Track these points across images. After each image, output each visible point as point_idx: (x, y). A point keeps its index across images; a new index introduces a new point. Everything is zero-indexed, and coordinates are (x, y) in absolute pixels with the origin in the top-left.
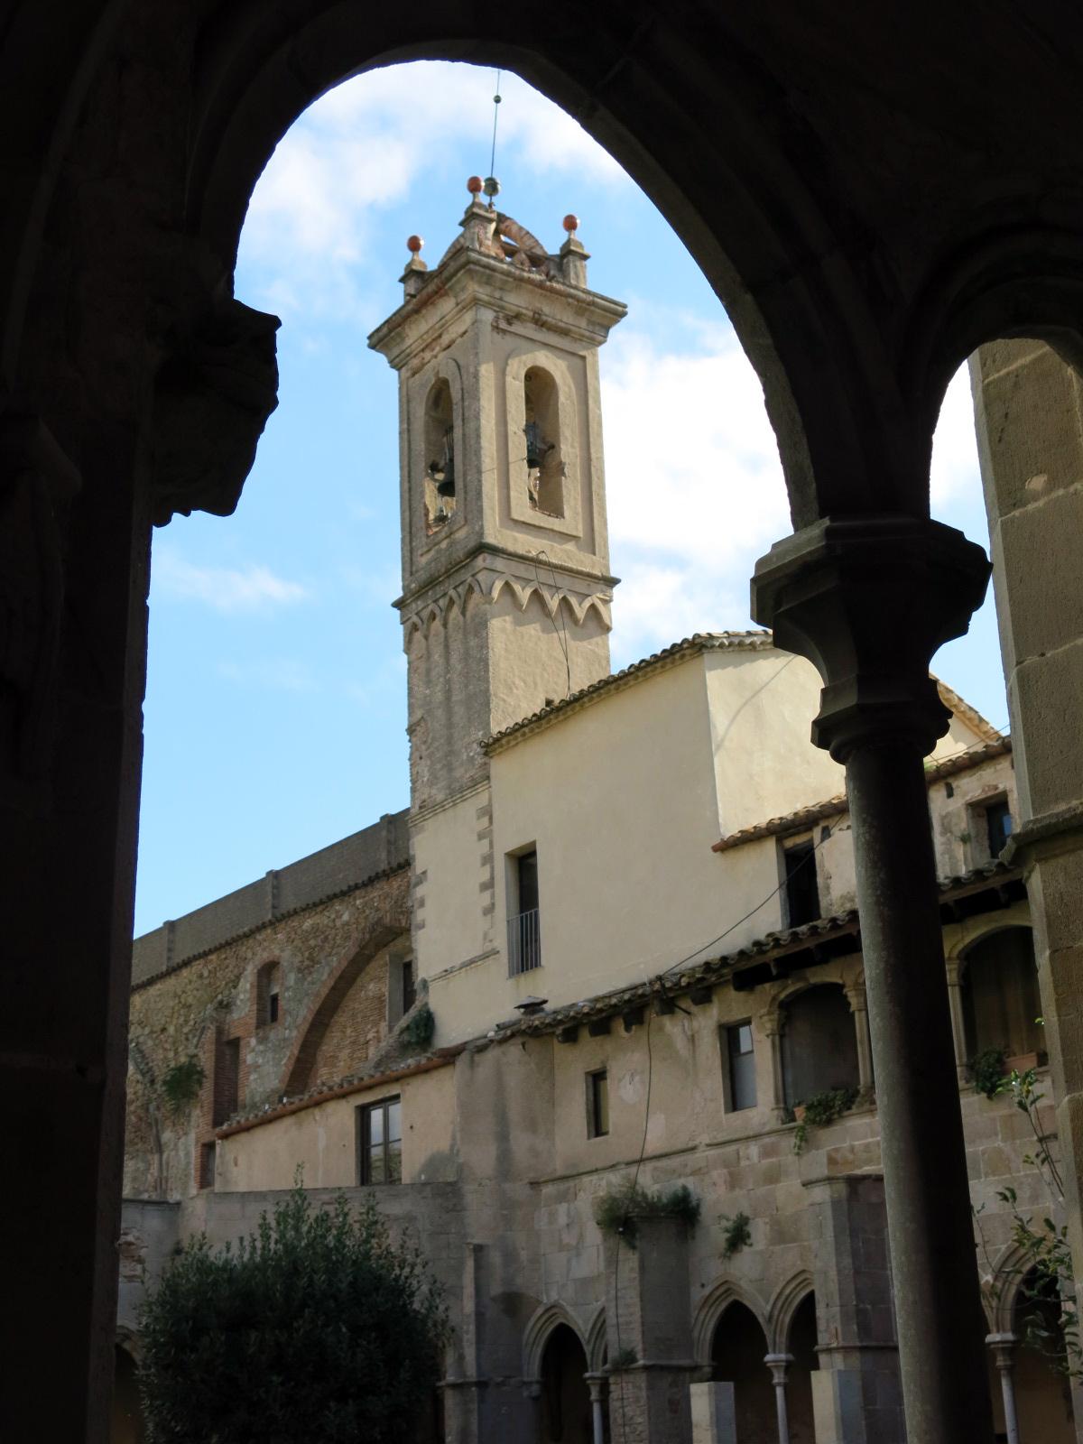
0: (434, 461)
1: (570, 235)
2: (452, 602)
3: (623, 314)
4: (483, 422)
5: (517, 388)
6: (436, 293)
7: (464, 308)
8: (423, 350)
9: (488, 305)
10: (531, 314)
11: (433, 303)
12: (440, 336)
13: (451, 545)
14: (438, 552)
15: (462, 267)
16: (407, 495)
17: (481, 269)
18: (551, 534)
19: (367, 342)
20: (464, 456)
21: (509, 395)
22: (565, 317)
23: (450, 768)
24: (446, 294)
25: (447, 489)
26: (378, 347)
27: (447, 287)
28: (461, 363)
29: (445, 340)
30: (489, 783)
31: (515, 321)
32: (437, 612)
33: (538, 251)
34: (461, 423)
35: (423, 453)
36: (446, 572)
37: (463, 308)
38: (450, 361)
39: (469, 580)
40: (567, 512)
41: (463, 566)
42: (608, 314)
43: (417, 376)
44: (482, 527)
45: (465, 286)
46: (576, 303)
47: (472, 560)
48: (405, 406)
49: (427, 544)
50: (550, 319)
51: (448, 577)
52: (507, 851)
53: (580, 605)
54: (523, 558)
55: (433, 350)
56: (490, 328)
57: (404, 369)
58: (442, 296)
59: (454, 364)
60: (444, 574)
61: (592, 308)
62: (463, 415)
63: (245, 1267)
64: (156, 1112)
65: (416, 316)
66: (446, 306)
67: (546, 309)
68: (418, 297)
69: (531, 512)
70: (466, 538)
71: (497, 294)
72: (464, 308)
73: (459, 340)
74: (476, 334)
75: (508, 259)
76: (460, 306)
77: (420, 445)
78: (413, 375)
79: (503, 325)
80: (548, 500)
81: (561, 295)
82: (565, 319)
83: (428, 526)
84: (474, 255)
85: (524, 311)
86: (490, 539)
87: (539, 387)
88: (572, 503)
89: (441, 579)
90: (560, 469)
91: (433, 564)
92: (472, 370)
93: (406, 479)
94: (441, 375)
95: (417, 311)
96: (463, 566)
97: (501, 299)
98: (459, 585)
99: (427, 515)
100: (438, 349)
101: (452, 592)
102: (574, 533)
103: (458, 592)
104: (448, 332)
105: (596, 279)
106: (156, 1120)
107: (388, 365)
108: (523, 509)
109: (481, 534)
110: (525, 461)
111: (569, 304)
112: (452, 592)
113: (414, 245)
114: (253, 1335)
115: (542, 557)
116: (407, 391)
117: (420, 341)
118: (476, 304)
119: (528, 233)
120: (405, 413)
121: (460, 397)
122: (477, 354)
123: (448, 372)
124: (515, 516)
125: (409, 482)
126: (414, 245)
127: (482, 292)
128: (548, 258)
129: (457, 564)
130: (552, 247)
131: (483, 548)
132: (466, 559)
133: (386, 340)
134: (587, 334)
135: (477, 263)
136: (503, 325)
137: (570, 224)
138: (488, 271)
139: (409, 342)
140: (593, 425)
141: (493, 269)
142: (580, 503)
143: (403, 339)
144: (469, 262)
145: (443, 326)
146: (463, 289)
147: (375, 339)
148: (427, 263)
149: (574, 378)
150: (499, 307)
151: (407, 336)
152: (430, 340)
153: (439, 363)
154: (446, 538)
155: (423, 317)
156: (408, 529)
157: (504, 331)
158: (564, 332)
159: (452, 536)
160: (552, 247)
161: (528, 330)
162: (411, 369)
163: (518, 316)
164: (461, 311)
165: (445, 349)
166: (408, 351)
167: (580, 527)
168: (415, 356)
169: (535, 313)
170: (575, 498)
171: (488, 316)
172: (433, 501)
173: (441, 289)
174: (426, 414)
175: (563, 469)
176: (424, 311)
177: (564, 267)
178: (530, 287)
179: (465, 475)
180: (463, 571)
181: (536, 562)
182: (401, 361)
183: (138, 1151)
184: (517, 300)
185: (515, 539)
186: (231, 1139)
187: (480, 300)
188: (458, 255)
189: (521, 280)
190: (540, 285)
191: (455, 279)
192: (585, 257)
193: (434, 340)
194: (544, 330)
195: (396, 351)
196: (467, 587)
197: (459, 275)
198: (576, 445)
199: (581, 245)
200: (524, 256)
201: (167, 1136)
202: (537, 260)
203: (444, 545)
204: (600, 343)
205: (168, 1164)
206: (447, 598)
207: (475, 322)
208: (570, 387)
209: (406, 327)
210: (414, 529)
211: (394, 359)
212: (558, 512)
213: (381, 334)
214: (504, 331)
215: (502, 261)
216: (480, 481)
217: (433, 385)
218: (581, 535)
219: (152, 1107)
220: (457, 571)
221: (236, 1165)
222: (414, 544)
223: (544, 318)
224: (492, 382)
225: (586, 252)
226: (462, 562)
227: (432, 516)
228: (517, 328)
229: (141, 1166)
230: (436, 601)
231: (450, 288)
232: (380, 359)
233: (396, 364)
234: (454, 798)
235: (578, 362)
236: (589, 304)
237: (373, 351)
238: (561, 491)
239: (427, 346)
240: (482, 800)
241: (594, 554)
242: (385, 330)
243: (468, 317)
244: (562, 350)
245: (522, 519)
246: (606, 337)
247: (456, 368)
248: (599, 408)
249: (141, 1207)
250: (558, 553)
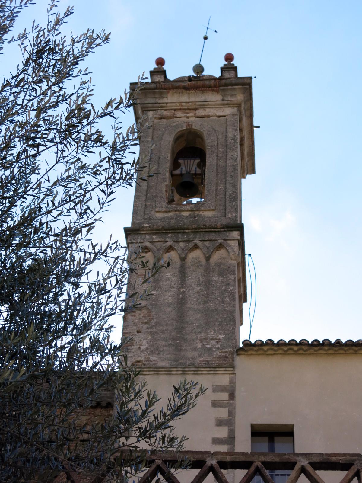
6: (210, 87)
7: (227, 104)
11: (203, 91)
12: (195, 109)
23: (178, 348)
24: (217, 92)
30: (234, 370)
36: (195, 229)
39: (220, 241)
45: (235, 95)
52: (254, 422)
58: (213, 91)
60: (192, 229)
65: (184, 91)
72: (227, 104)
95: (186, 88)
132: (221, 228)
139: (165, 100)
143: (163, 98)
145: (204, 105)
155: (189, 94)
164: (224, 104)
168: (166, 110)
182: (153, 107)
209: (171, 92)
226: (216, 228)
234: (186, 369)
240: (224, 379)
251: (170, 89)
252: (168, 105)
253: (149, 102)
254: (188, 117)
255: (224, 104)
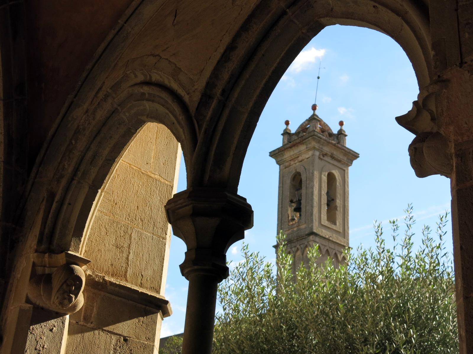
0: (292, 199)
1: (341, 127)
2: (298, 249)
3: (359, 157)
4: (314, 190)
5: (325, 178)
6: (299, 143)
7: (309, 149)
8: (290, 160)
9: (318, 150)
10: (330, 154)
11: (297, 146)
12: (298, 157)
13: (298, 230)
14: (292, 231)
15: (312, 136)
16: (280, 209)
17: (318, 138)
18: (332, 230)
19: (269, 154)
20: (306, 200)
21: (322, 181)
22: (340, 156)
24: (303, 144)
25: (298, 209)
26: (273, 156)
27: (304, 142)
28: (306, 168)
29: (300, 159)
31: (325, 156)
32: (291, 252)
33: (331, 132)
34: (305, 189)
35: (288, 196)
36: (297, 239)
37: (308, 150)
38: (302, 166)
39: (306, 243)
40: (338, 224)
41: (304, 238)
42: (354, 157)
43: (287, 169)
44: (312, 226)
46: (344, 152)
47: (308, 237)
48: (282, 178)
49: (288, 228)
50: (336, 157)
51: (297, 241)
53: (340, 255)
54: (324, 238)
55: (295, 161)
56: (318, 158)
57: (282, 166)
58: (301, 144)
59: (303, 167)
61: (349, 154)
62: (306, 186)
66: (303, 148)
67: (335, 153)
68: (292, 143)
69: (327, 222)
70: (305, 228)
71: (321, 147)
72: (309, 149)
73: (306, 160)
74: (314, 159)
75: (322, 133)
76: (308, 149)
77: (287, 193)
78: (286, 168)
79: (322, 157)
80: (332, 218)
81: (341, 149)
82: (340, 157)
83: (289, 222)
84: (316, 133)
85: (328, 153)
86: (315, 231)
87: (331, 178)
88: (339, 220)
89: (294, 241)
90: (336, 208)
91: (290, 235)
92: (311, 171)
93: (281, 203)
94: (298, 171)
95: (291, 147)
96: (304, 238)
97: (322, 148)
98: (301, 244)
99: (288, 217)
100: (297, 161)
101: (298, 246)
102: (339, 231)
103: (301, 247)
104: (301, 156)
105: (350, 143)
107: (276, 163)
108: (325, 222)
109: (312, 228)
110: (326, 205)
111: (342, 152)
112: (298, 246)
113: (287, 123)
115: (331, 238)
116: (283, 173)
117: (290, 157)
118: (314, 149)
119: (327, 125)
120: (282, 181)
121: (305, 179)
122: (313, 166)
123: (301, 170)
124: (322, 223)
125: (282, 205)
126: (287, 123)
127: (317, 145)
128: (334, 135)
129: (301, 237)
130: (335, 131)
131: (313, 233)
133: (277, 155)
134: (346, 162)
135: (316, 136)
136: (322, 157)
137: (341, 123)
138: (319, 139)
139: (285, 157)
140: (346, 194)
141: (321, 138)
142: (341, 220)
143: (283, 156)
144: (314, 135)
145: (300, 154)
146: (310, 143)
147: (272, 154)
148: (291, 130)
149: (341, 177)
150: (321, 151)
151: (285, 155)
152: (293, 158)
153: (296, 166)
154: (296, 227)
156: (280, 221)
157: (322, 159)
158: (339, 161)
159: (299, 227)
160: (335, 131)
161: (328, 159)
162: (285, 166)
163: (326, 154)
164: (308, 150)
165: (300, 162)
166: (285, 160)
167: (341, 229)
168: (287, 162)
169: (331, 154)
170: (340, 219)
171: (317, 153)
172: (290, 211)
173: (301, 142)
174: (290, 182)
175: (337, 208)
176: (293, 148)
177: (339, 138)
178: (331, 145)
179: (306, 207)
180: (304, 240)
181: (328, 240)
184: (327, 149)
185: (322, 231)
187: (315, 148)
188: (303, 129)
189: (329, 143)
190: (334, 145)
191: (307, 140)
192: (346, 136)
193: (296, 158)
194: (333, 159)
195: (279, 159)
196: (305, 246)
197: (309, 138)
198: (341, 200)
199: (344, 132)
200: (327, 133)
202: (331, 135)
203: (295, 229)
204: (350, 166)
206: (296, 249)
207: (313, 155)
208: (340, 180)
210: (282, 221)
211: (279, 161)
212: (335, 224)
213: (275, 153)
214: (322, 159)
215: (320, 134)
216: (312, 210)
217: (294, 174)
218: (341, 231)
220: (301, 239)
222: (282, 227)
223: (334, 156)
224: (318, 176)
225: (346, 133)
227: (290, 218)
228: (326, 158)
230: (291, 248)
231: (305, 142)
232: (273, 161)
233: (278, 163)
235: (342, 171)
236: (348, 153)
237: (271, 158)
238: (336, 216)
239: (292, 159)
241: (345, 238)
242: (277, 151)
243: (310, 153)
244: (338, 167)
245: (324, 224)
246: (352, 164)
247: (304, 170)
248: (348, 188)
250: (335, 238)
251: (284, 150)
252: (287, 159)
253: (279, 160)
254: (296, 164)
255: (308, 150)
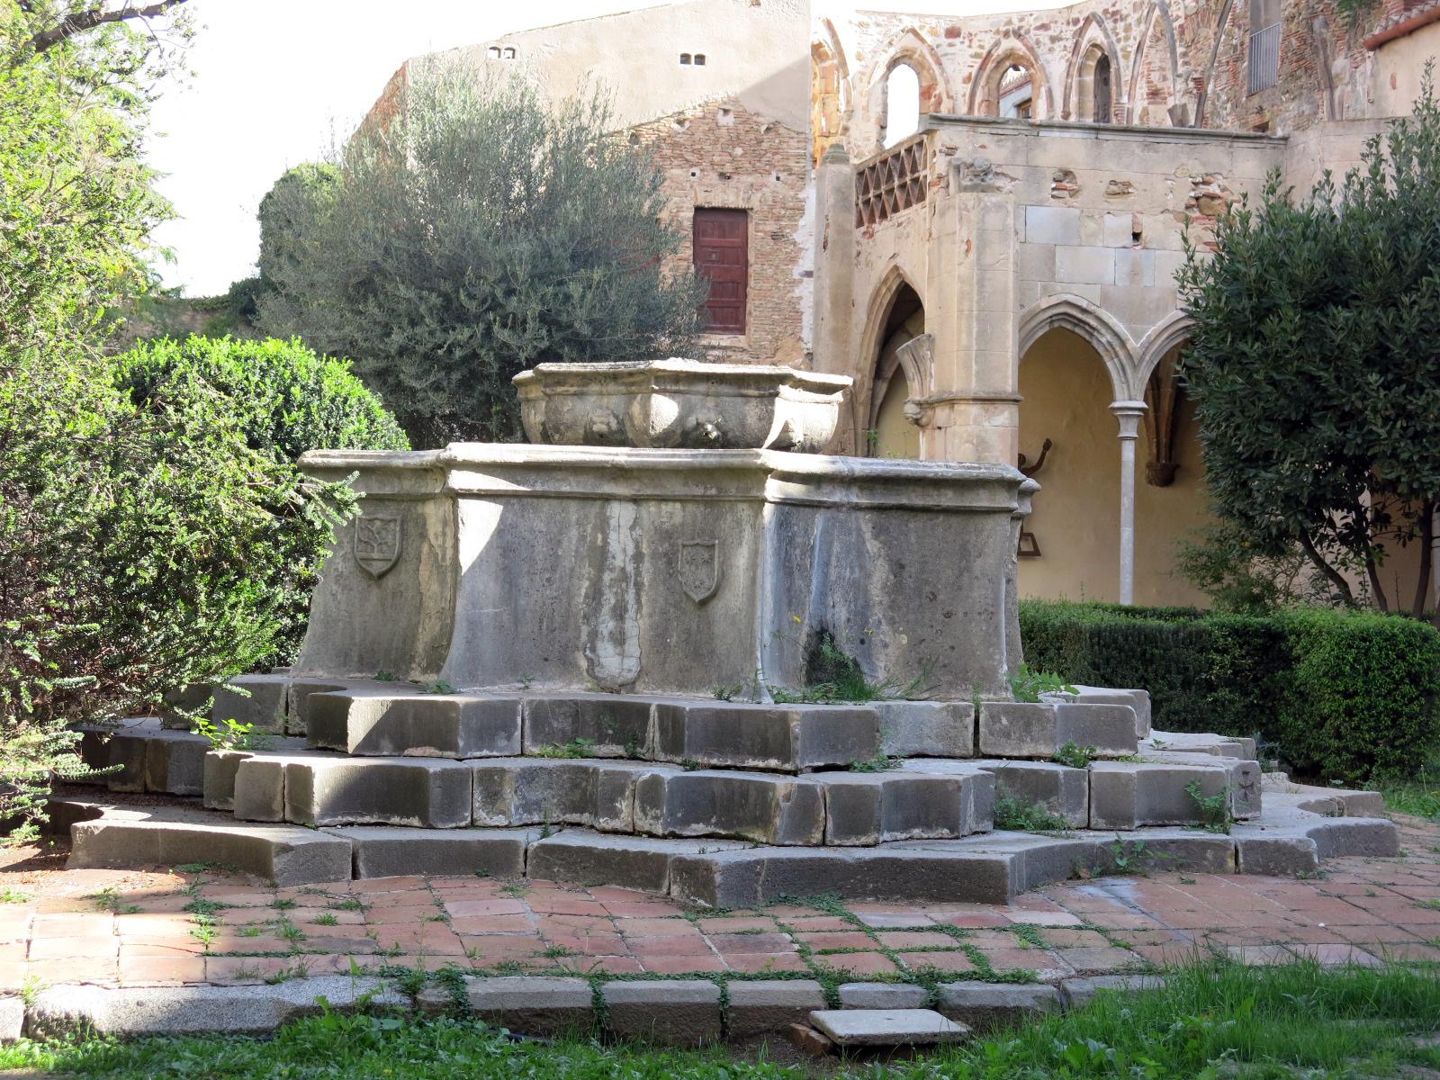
63: (1350, 216)
64: (1324, 31)
106: (1324, 42)
114: (1342, 314)
183: (1302, 87)
186: (1386, 49)
201: (1340, 64)
205: (1341, 104)
219: (1317, 23)
221: (1394, 88)
229: (1306, 108)
249: (1228, 143)
